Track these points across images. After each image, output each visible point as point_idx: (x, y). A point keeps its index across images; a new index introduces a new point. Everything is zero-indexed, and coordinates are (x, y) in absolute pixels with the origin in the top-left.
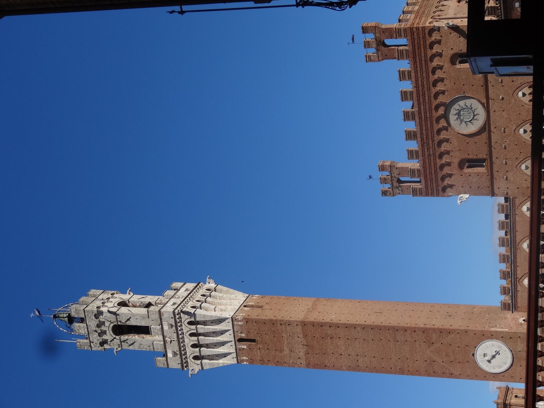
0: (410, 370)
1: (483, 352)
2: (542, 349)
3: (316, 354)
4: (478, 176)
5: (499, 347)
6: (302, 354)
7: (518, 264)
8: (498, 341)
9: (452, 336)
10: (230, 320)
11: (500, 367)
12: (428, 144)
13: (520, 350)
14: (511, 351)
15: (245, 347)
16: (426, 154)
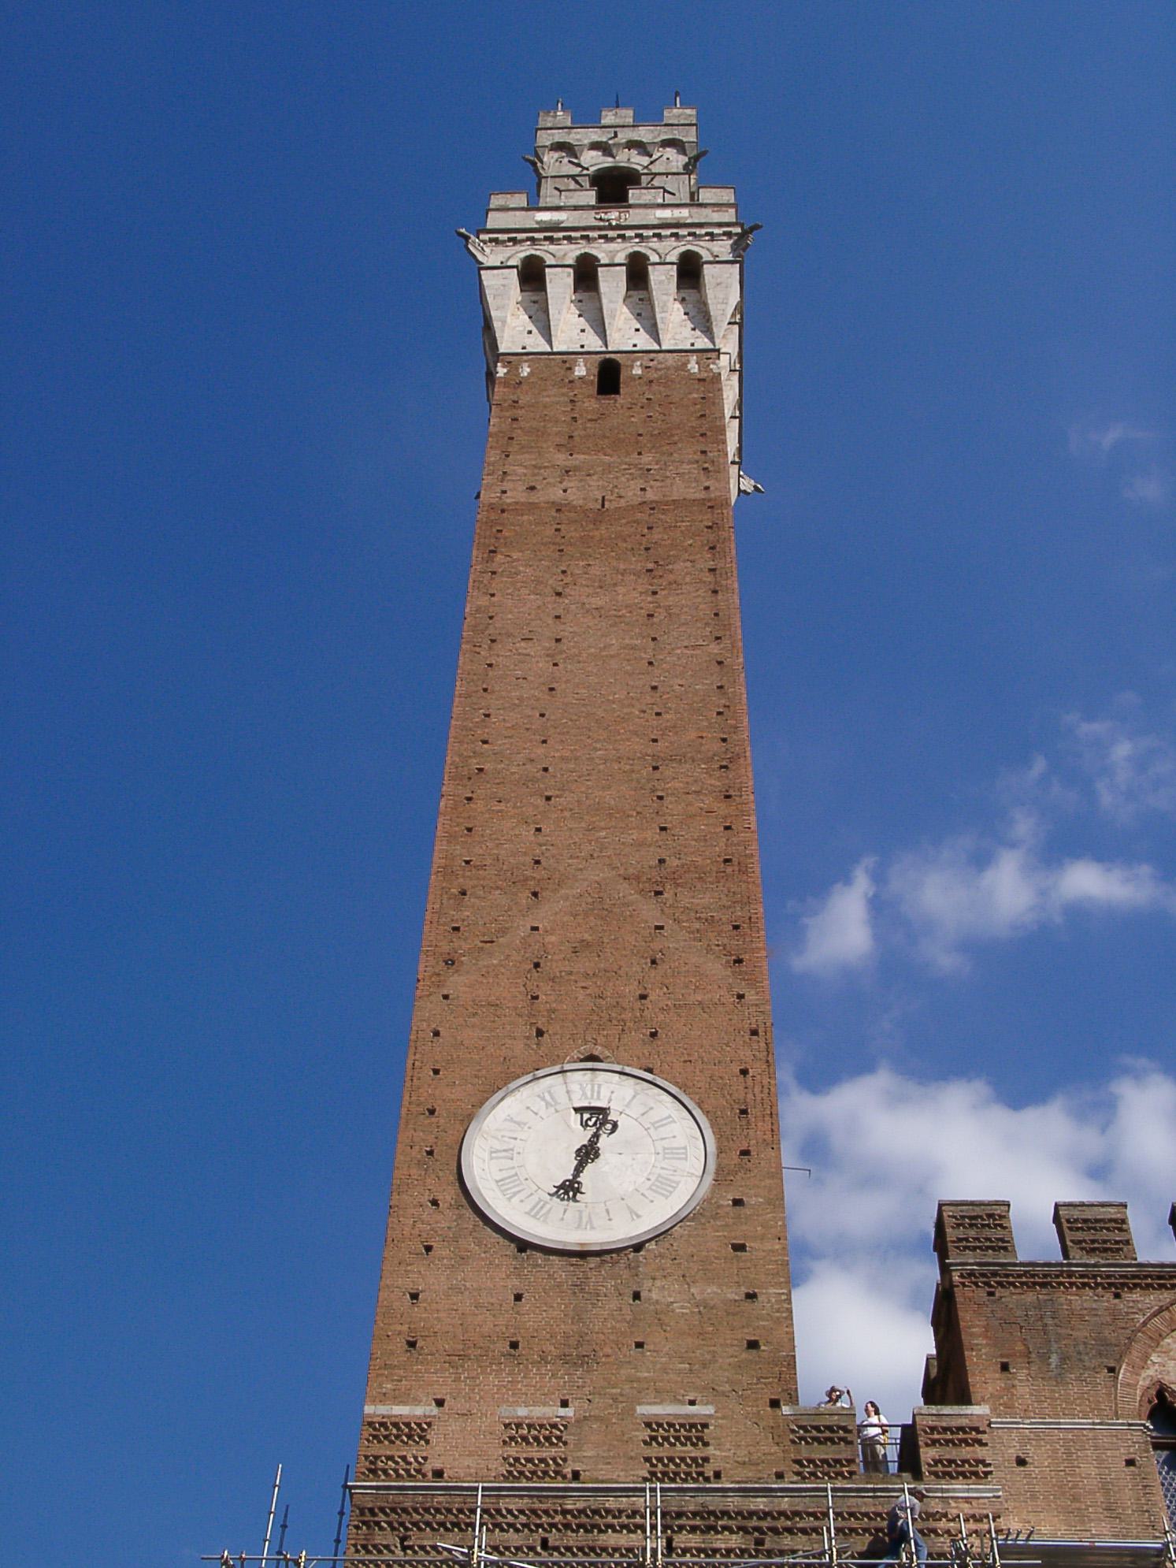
0: (479, 805)
2: (660, 1425)
5: (663, 1185)
8: (709, 1179)
9: (717, 968)
13: (654, 1293)
14: (638, 1247)
15: (580, 371)
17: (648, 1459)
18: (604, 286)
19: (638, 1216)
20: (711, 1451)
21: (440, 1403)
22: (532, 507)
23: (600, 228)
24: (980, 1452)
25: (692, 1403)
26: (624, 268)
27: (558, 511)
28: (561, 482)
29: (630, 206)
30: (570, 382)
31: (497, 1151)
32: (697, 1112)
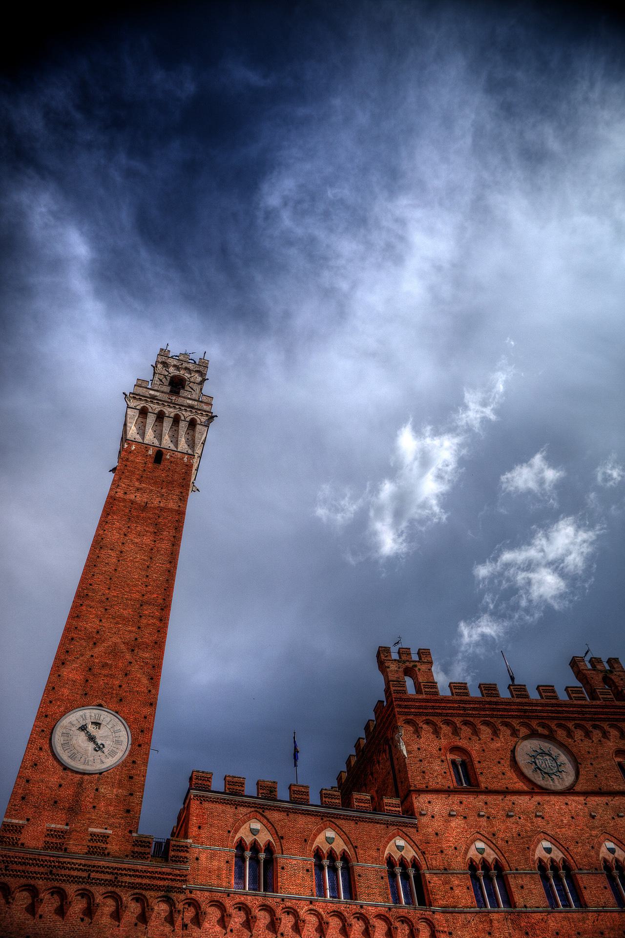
0: (84, 608)
1: (104, 723)
2: (95, 835)
3: (130, 511)
4: (445, 773)
5: (112, 753)
6: (132, 497)
7: (292, 816)
9: (145, 681)
10: (190, 452)
11: (66, 745)
12: (484, 710)
14: (101, 774)
15: (150, 452)
16: (467, 706)
17: (88, 846)
18: (165, 424)
19: (103, 763)
20: (109, 846)
21: (28, 820)
22: (124, 500)
23: (168, 402)
24: (188, 855)
25: (106, 829)
26: (172, 419)
27: (132, 504)
28: (135, 493)
29: (180, 396)
30: (147, 456)
31: (64, 734)
32: (128, 729)
